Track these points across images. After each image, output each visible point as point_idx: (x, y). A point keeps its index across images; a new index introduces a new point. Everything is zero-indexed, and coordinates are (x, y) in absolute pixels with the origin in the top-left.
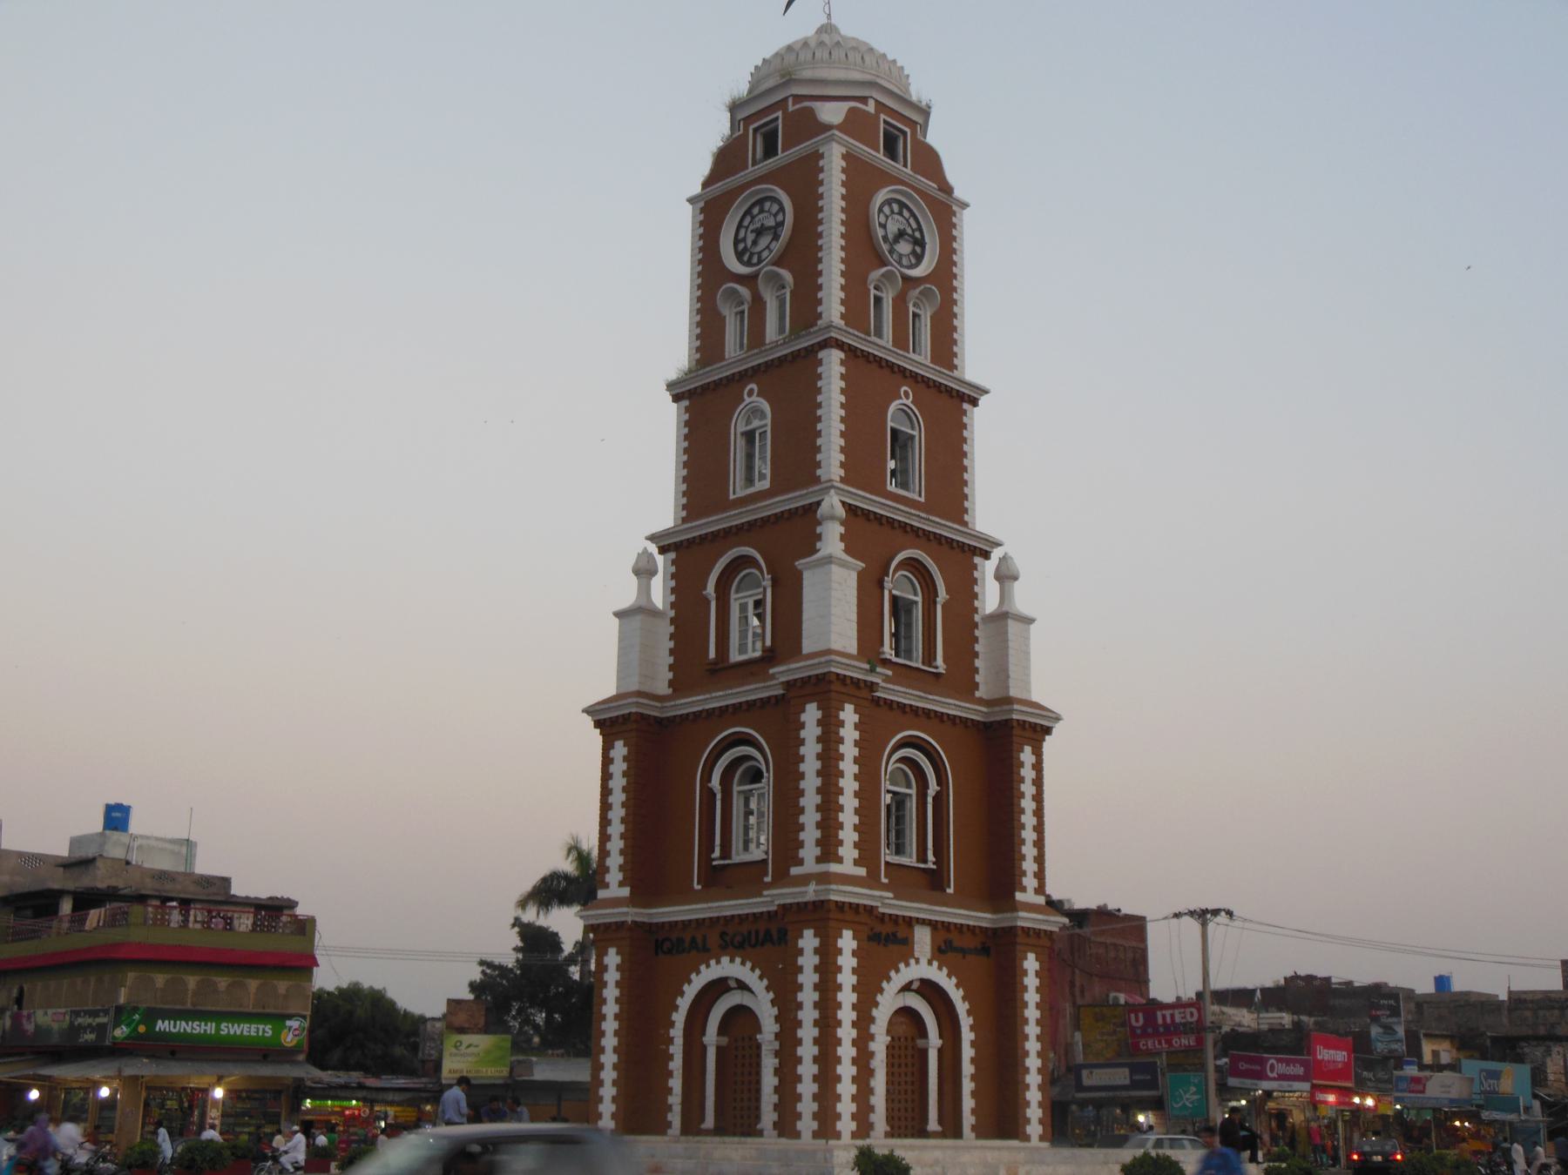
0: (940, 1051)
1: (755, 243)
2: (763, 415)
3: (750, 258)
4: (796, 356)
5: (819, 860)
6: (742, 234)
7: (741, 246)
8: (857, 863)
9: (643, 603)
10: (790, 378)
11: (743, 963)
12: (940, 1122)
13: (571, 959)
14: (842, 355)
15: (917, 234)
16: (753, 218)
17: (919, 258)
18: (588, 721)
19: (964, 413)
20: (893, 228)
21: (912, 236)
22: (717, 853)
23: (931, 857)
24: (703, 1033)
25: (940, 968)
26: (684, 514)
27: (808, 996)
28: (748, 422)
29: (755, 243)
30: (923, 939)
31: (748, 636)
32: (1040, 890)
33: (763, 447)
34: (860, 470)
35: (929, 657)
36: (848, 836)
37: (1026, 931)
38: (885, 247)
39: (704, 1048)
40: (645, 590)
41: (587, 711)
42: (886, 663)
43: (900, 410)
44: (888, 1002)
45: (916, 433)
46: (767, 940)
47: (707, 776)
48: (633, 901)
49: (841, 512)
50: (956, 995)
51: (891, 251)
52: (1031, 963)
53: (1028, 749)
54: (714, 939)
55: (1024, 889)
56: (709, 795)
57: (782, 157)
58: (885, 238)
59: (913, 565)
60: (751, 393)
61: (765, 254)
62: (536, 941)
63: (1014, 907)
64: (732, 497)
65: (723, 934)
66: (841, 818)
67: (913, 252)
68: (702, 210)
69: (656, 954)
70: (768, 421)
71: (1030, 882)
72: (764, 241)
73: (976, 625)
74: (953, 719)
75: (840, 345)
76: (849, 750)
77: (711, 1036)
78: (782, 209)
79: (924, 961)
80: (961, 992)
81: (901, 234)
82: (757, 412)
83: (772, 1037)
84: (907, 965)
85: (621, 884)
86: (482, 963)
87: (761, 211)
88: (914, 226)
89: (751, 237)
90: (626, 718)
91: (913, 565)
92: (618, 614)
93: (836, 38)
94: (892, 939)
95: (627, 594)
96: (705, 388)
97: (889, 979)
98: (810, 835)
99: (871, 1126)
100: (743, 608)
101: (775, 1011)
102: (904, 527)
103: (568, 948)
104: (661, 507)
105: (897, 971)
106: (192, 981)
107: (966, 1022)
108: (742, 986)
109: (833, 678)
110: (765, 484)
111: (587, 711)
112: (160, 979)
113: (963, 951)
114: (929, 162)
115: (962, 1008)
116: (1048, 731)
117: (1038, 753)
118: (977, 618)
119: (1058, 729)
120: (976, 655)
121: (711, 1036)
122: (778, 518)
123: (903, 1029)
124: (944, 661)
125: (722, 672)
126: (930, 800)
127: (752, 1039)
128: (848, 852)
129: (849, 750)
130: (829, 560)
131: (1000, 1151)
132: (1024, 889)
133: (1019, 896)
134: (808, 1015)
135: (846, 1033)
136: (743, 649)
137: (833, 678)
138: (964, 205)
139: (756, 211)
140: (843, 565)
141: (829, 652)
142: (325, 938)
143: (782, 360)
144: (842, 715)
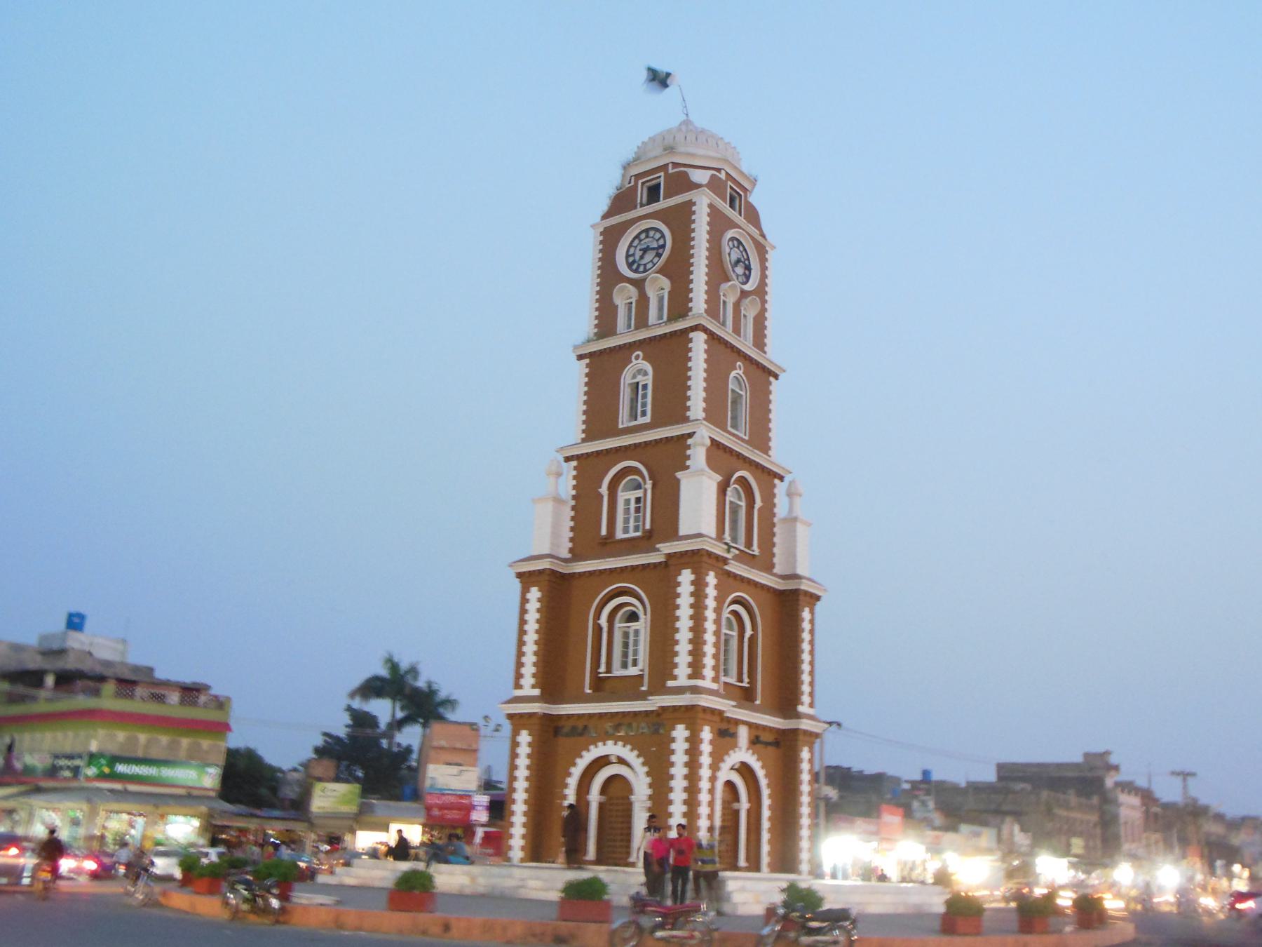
0: (749, 811)
1: (642, 257)
2: (646, 374)
4: (673, 334)
5: (690, 677)
6: (632, 251)
12: (748, 859)
13: (384, 735)
23: (746, 679)
24: (588, 793)
28: (634, 377)
29: (642, 257)
30: (743, 734)
33: (644, 396)
34: (715, 415)
35: (749, 544)
36: (709, 661)
45: (743, 393)
50: (760, 773)
53: (807, 610)
56: (598, 629)
61: (649, 266)
62: (362, 720)
63: (798, 716)
71: (806, 699)
72: (649, 256)
74: (763, 586)
78: (663, 236)
86: (326, 734)
87: (647, 237)
98: (683, 659)
106: (143, 737)
108: (621, 761)
112: (121, 736)
115: (763, 782)
116: (818, 598)
124: (759, 547)
125: (609, 545)
139: (643, 236)
141: (700, 535)
142: (236, 716)
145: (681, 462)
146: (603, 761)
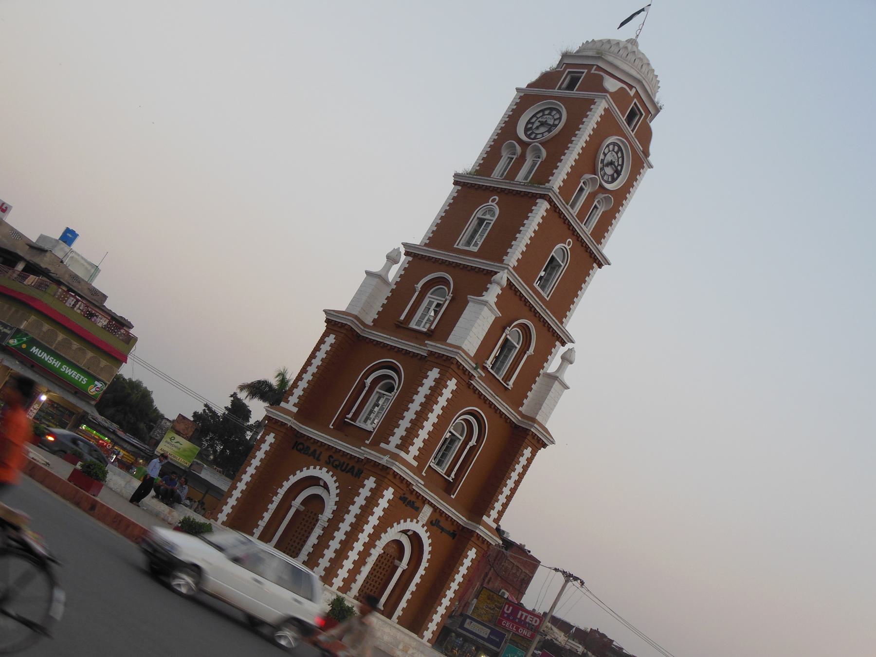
1: (537, 128)
2: (493, 215)
3: (531, 134)
4: (526, 194)
5: (397, 447)
6: (533, 120)
7: (530, 126)
8: (415, 458)
9: (383, 274)
10: (518, 203)
11: (332, 476)
13: (250, 428)
14: (549, 207)
15: (619, 168)
16: (544, 115)
17: (614, 180)
18: (324, 317)
19: (592, 268)
20: (609, 158)
21: (616, 167)
22: (350, 416)
23: (453, 475)
25: (426, 531)
26: (427, 242)
27: (355, 510)
28: (484, 214)
29: (537, 128)
30: (426, 512)
31: (424, 319)
32: (497, 521)
33: (485, 230)
34: (525, 268)
35: (507, 378)
36: (418, 443)
37: (479, 536)
38: (600, 166)
39: (291, 506)
40: (387, 269)
41: (326, 312)
42: (484, 368)
43: (561, 249)
44: (392, 533)
46: (351, 471)
47: (366, 376)
48: (297, 416)
49: (504, 283)
50: (427, 549)
51: (602, 169)
52: (472, 554)
53: (530, 449)
54: (325, 456)
55: (489, 516)
57: (575, 93)
58: (602, 161)
59: (525, 328)
60: (493, 201)
61: (539, 136)
62: (238, 409)
63: (479, 521)
64: (455, 246)
65: (330, 456)
66: (419, 432)
67: (612, 176)
68: (521, 98)
69: (293, 447)
70: (494, 219)
71: (494, 514)
72: (542, 130)
73: (539, 375)
74: (501, 414)
75: (550, 201)
76: (442, 401)
77: (297, 503)
78: (560, 119)
79: (420, 524)
80: (430, 549)
81: (611, 163)
82: (491, 211)
83: (326, 519)
84: (411, 521)
85: (295, 405)
86: (206, 405)
88: (620, 163)
89: (537, 124)
90: (343, 325)
91: (525, 328)
92: (367, 272)
93: (635, 49)
94: (411, 504)
95: (377, 266)
96: (472, 186)
97: (399, 523)
98: (400, 432)
99: (350, 589)
100: (430, 303)
101: (335, 508)
102: (531, 307)
103: (252, 421)
104: (417, 232)
105: (405, 521)
106: (61, 336)
107: (424, 564)
108: (326, 486)
109: (455, 362)
110: (476, 249)
111: (326, 312)
112: (46, 327)
113: (442, 529)
114: (646, 136)
115: (426, 556)
116: (544, 445)
117: (534, 454)
118: (541, 372)
119: (550, 447)
120: (531, 390)
121: (297, 503)
122: (473, 269)
123: (392, 551)
125: (402, 328)
126: (468, 447)
127: (316, 515)
128: (414, 450)
129: (442, 401)
130: (485, 303)
131: (406, 636)
132: (489, 516)
133: (485, 518)
134: (350, 518)
135: (363, 538)
136: (419, 323)
137: (455, 362)
138: (651, 166)
139: (547, 112)
140: (491, 310)
141: (459, 348)
142: (137, 350)
143: (518, 193)
144: (449, 383)
145: (481, 290)
146: (314, 481)
